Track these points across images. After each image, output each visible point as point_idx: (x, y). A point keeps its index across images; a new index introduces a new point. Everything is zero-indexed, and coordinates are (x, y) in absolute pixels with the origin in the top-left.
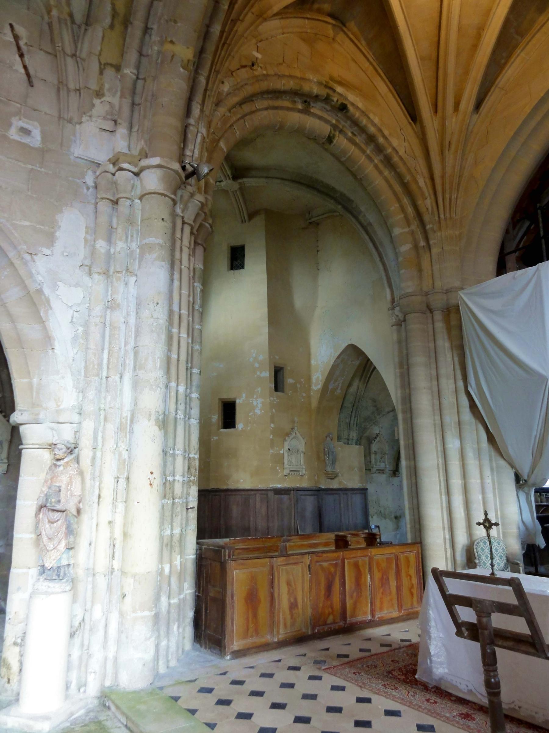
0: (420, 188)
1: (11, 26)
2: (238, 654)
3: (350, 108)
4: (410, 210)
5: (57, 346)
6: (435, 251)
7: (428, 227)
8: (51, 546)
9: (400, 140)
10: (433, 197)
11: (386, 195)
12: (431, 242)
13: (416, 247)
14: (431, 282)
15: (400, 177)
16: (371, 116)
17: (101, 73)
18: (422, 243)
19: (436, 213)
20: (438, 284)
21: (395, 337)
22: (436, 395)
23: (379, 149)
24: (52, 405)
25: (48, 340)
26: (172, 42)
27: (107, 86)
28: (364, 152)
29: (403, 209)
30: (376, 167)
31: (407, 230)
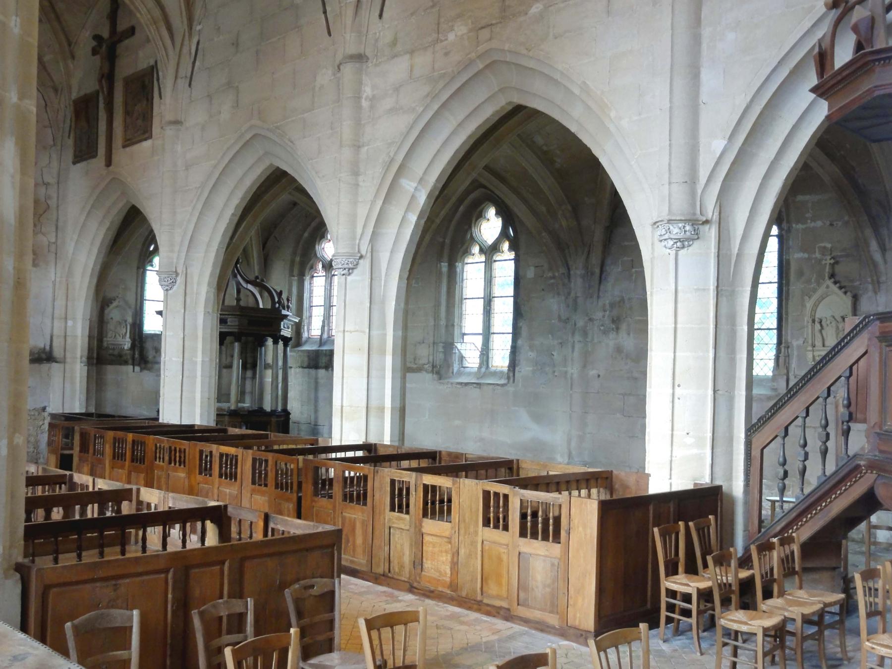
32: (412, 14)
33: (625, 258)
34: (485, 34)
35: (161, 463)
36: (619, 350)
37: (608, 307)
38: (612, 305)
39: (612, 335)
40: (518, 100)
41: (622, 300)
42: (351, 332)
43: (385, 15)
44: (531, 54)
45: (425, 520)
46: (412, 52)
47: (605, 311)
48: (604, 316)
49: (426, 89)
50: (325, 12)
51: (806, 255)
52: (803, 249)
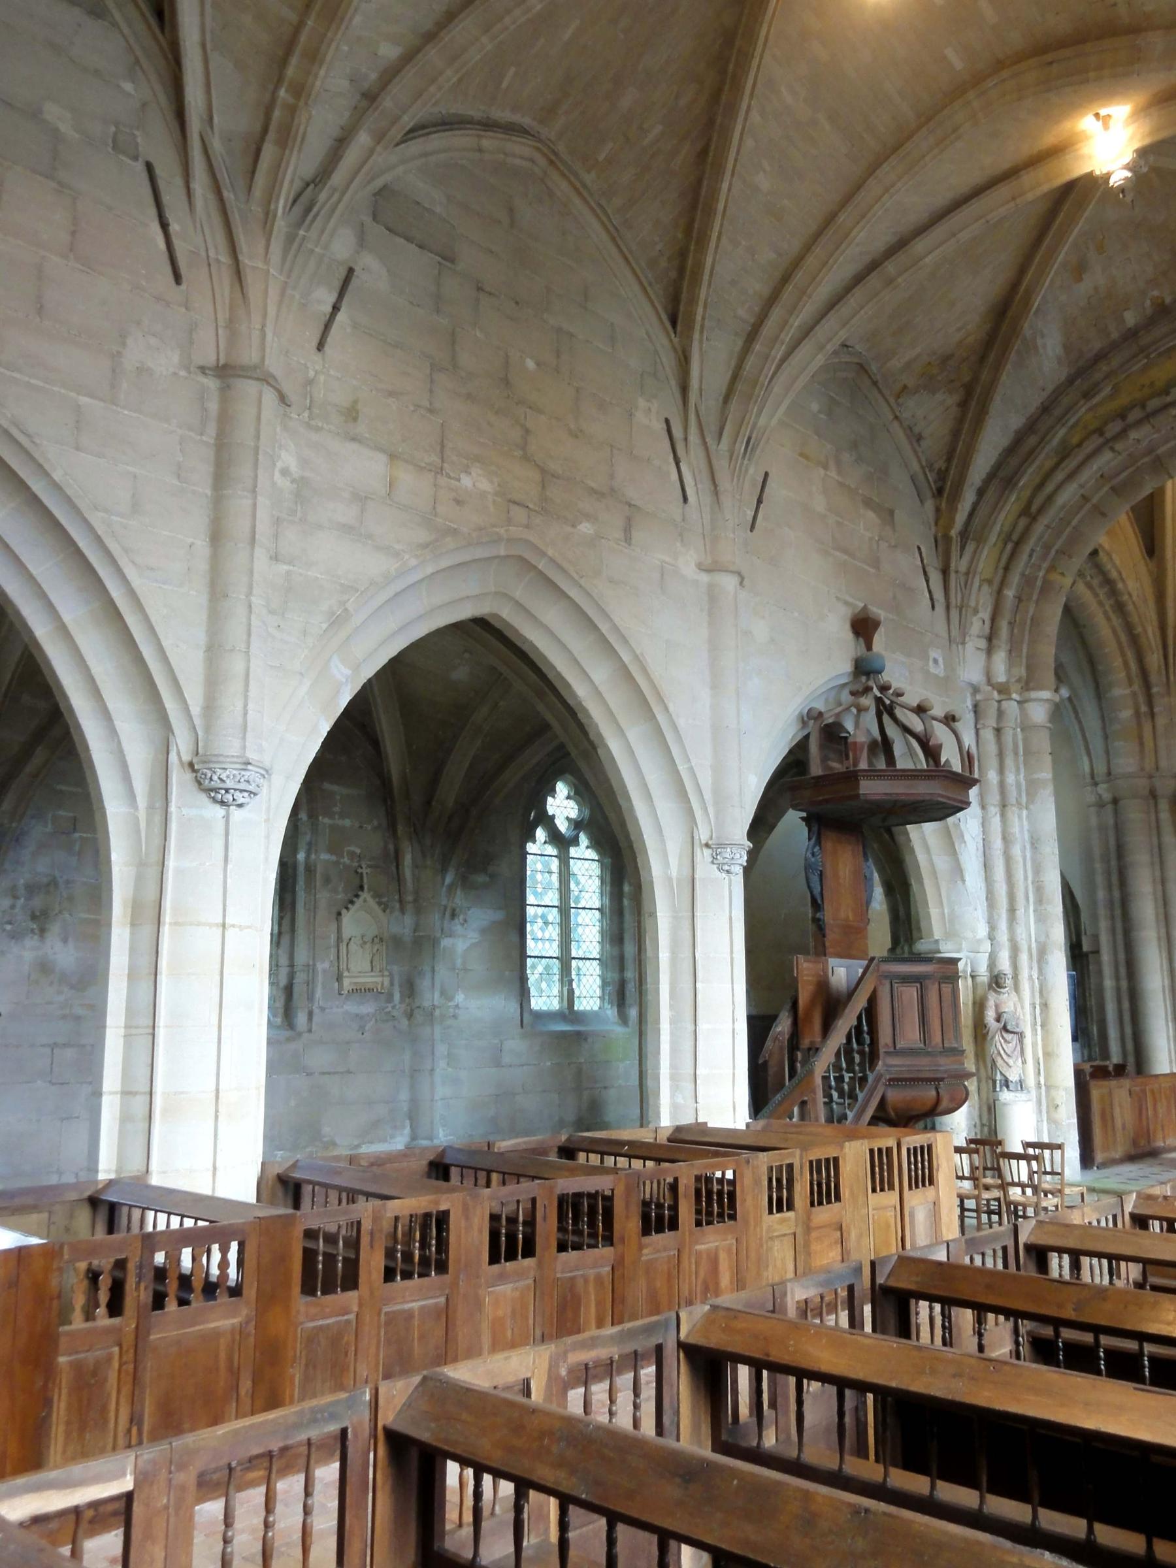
0: (1147, 638)
1: (919, 548)
2: (1104, 1165)
3: (1101, 553)
4: (1133, 666)
5: (967, 878)
6: (1161, 721)
7: (1155, 690)
8: (1011, 1062)
9: (1134, 580)
10: (1161, 652)
11: (1111, 647)
12: (1156, 710)
13: (1137, 713)
14: (1153, 759)
15: (1129, 627)
16: (1114, 556)
17: (980, 586)
18: (1144, 708)
19: (1164, 672)
20: (1163, 764)
21: (1094, 821)
22: (1161, 902)
23: (1113, 592)
24: (969, 935)
25: (958, 871)
26: (1062, 574)
27: (981, 602)
28: (1096, 595)
29: (1126, 663)
30: (1105, 613)
31: (1127, 691)
32: (391, 394)
33: (61, 813)
34: (519, 514)
35: (103, 1319)
36: (44, 967)
37: (21, 891)
38: (32, 889)
39: (31, 942)
40: (507, 614)
41: (53, 883)
42: (241, 928)
43: (327, 348)
44: (582, 582)
45: (813, 1209)
46: (393, 457)
47: (16, 897)
48: (13, 907)
49: (423, 536)
50: (164, 226)
51: (334, 858)
52: (331, 850)
